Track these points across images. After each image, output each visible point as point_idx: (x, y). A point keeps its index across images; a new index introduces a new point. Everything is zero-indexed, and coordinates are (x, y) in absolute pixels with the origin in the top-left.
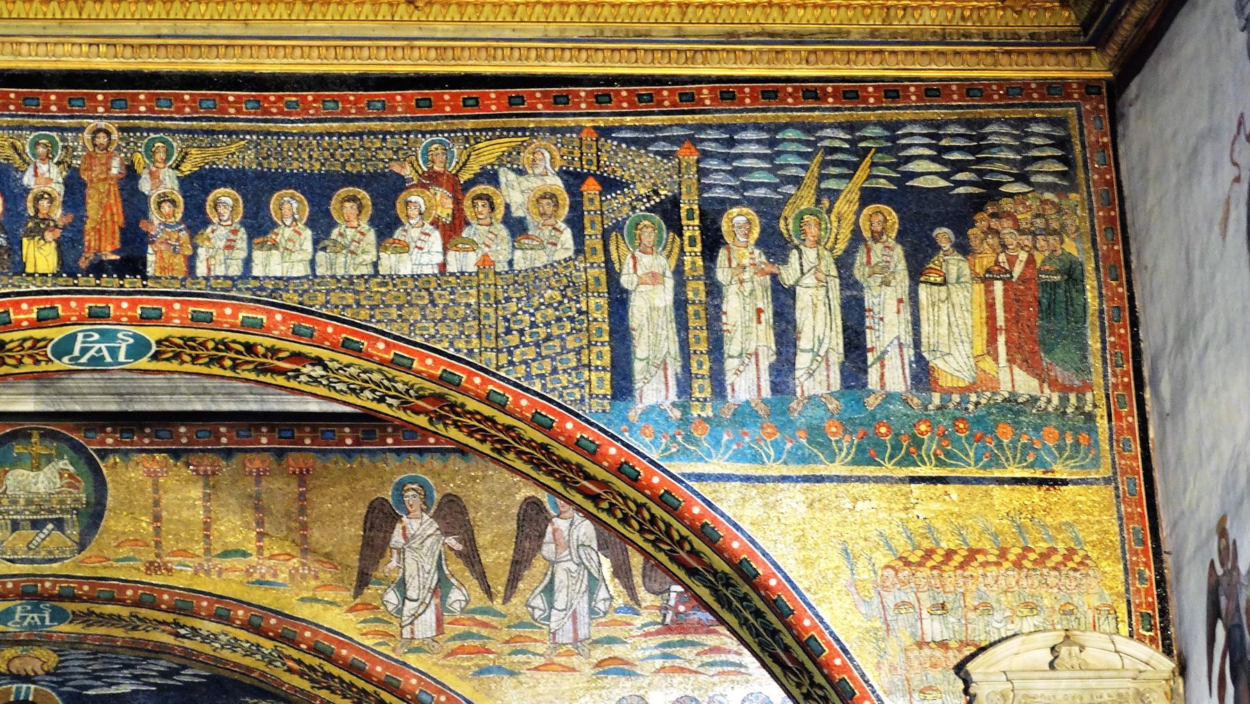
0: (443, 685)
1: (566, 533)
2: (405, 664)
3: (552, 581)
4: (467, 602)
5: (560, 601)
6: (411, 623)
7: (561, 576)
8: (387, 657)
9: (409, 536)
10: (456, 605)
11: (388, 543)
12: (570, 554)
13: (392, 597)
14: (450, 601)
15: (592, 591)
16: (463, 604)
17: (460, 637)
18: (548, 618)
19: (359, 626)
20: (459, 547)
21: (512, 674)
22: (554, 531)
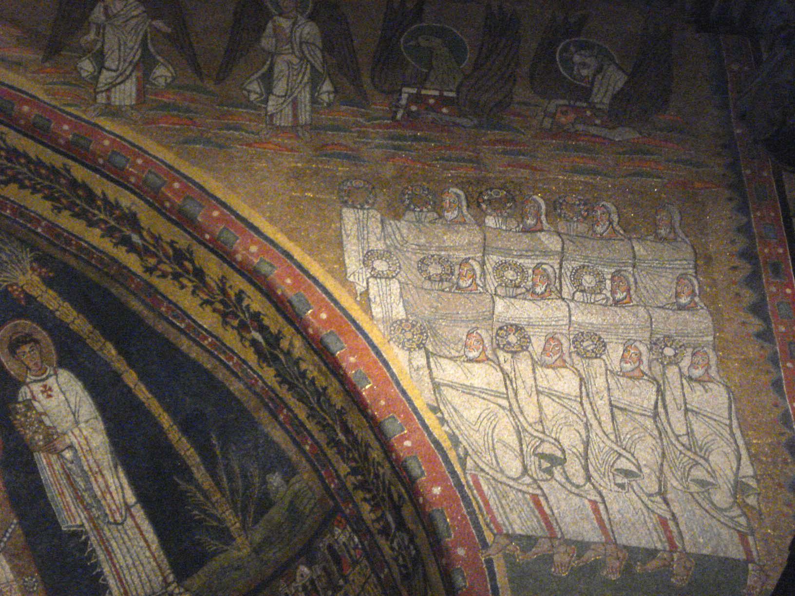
0: (140, 149)
1: (288, 31)
2: (95, 125)
3: (271, 69)
4: (174, 79)
5: (280, 87)
6: (108, 90)
7: (280, 66)
8: (76, 117)
9: (111, 15)
10: (162, 81)
11: (87, 18)
12: (292, 48)
13: (87, 66)
14: (153, 76)
15: (315, 84)
16: (169, 80)
17: (165, 107)
18: (266, 101)
19: (45, 87)
20: (169, 30)
21: (221, 147)
22: (275, 29)
